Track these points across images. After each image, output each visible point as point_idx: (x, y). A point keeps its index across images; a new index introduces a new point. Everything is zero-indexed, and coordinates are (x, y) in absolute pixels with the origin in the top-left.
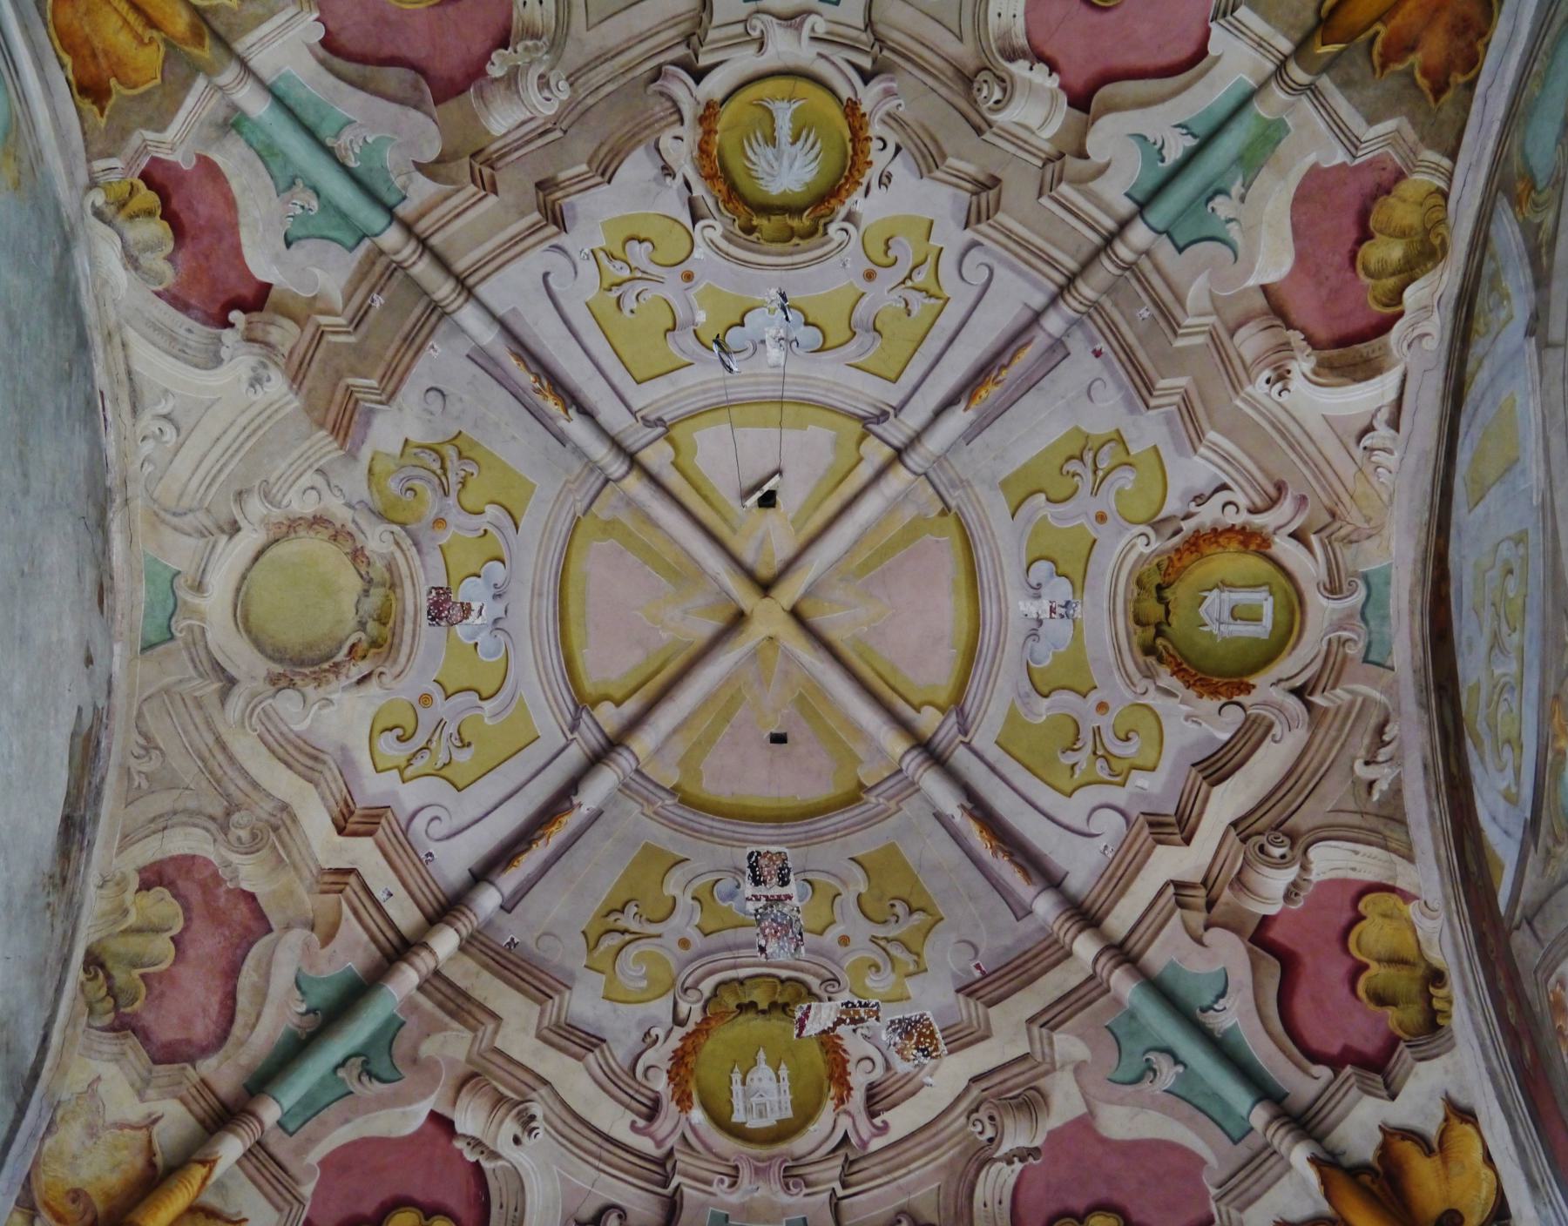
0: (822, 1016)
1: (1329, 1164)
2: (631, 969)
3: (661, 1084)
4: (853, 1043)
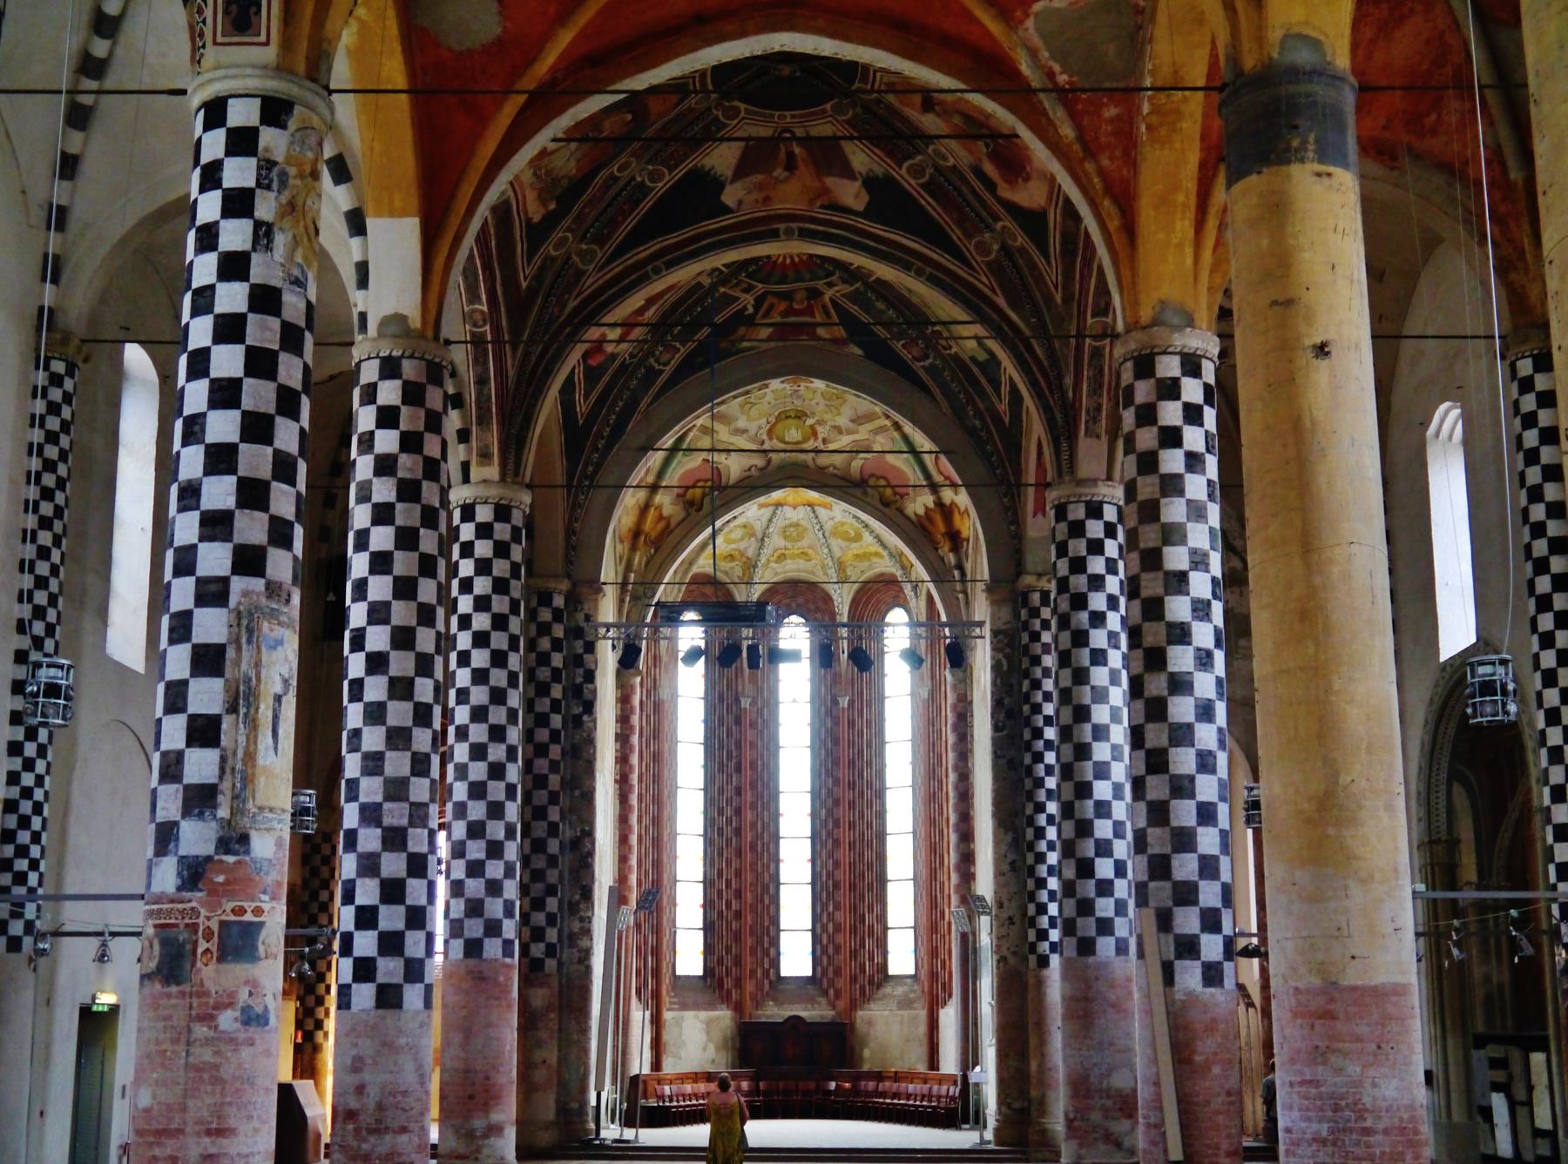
0: (810, 422)
1: (939, 504)
2: (754, 412)
3: (765, 437)
4: (820, 429)
